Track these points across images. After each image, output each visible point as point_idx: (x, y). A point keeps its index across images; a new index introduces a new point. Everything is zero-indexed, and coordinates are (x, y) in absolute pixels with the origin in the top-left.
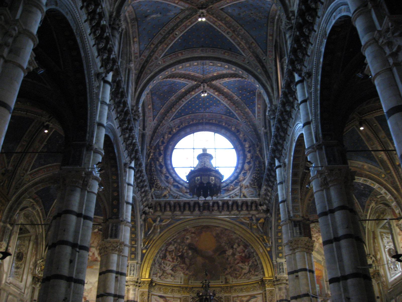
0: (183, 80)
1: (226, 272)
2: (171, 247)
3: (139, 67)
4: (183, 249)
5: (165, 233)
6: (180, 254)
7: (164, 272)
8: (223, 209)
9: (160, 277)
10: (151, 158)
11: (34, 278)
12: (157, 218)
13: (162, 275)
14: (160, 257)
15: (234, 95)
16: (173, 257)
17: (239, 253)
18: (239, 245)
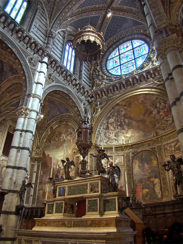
0: (95, 14)
1: (156, 128)
2: (110, 120)
3: (51, 9)
4: (121, 120)
5: (103, 110)
6: (119, 123)
7: (109, 138)
8: (141, 81)
9: (106, 143)
10: (93, 70)
11: (31, 159)
12: (97, 103)
13: (108, 141)
14: (104, 128)
15: (132, 8)
16: (114, 127)
17: (163, 110)
18: (160, 104)
